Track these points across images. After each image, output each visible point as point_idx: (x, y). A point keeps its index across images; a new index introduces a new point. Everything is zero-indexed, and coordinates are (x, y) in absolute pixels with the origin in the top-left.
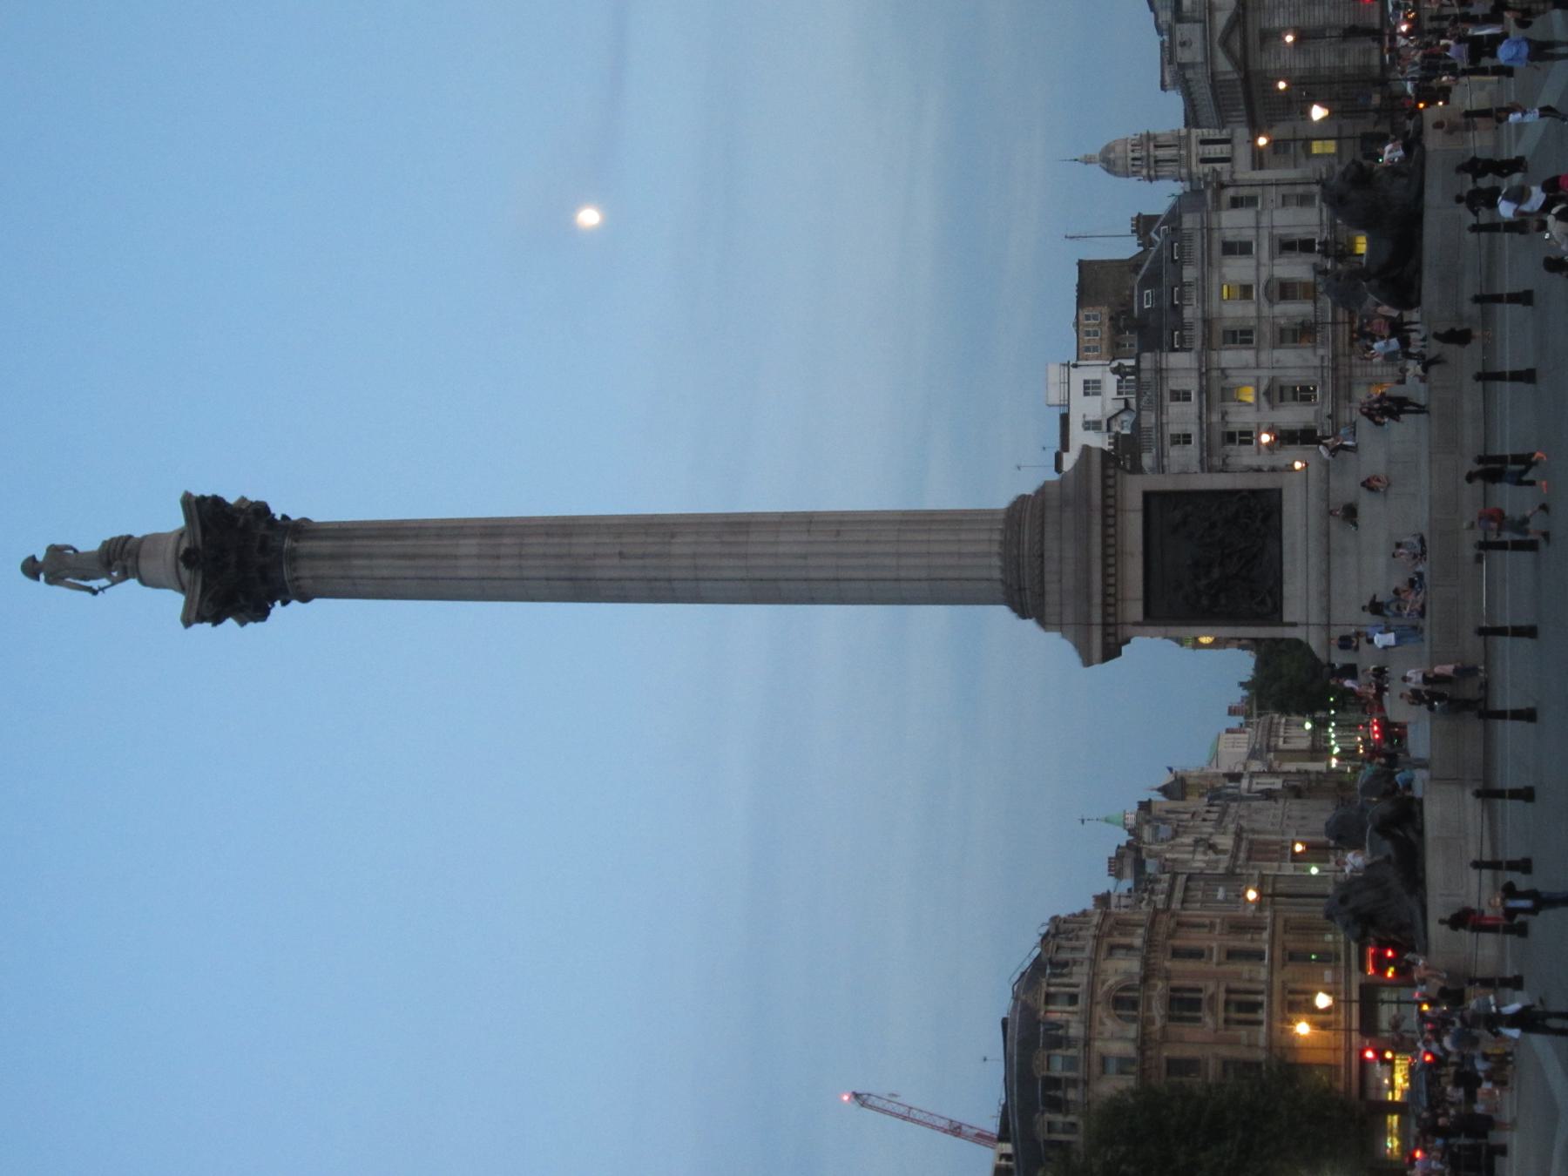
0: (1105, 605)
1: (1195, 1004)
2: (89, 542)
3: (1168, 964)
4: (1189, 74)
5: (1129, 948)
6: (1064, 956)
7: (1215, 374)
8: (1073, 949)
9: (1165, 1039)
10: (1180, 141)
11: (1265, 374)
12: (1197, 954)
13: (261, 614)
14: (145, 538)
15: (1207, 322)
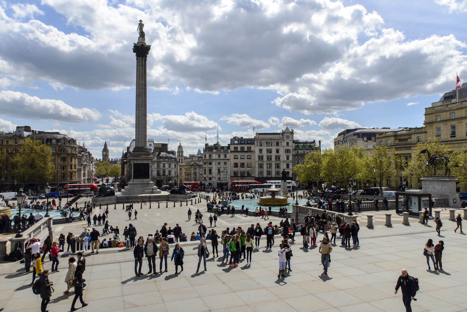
0: (136, 159)
1: (64, 160)
2: (145, 30)
3: (70, 157)
4: (191, 159)
5: (72, 151)
6: (71, 142)
7: (154, 163)
8: (72, 143)
9: (58, 157)
10: (182, 156)
11: (153, 169)
12: (71, 160)
13: (134, 52)
14: (145, 38)
15: (160, 162)
